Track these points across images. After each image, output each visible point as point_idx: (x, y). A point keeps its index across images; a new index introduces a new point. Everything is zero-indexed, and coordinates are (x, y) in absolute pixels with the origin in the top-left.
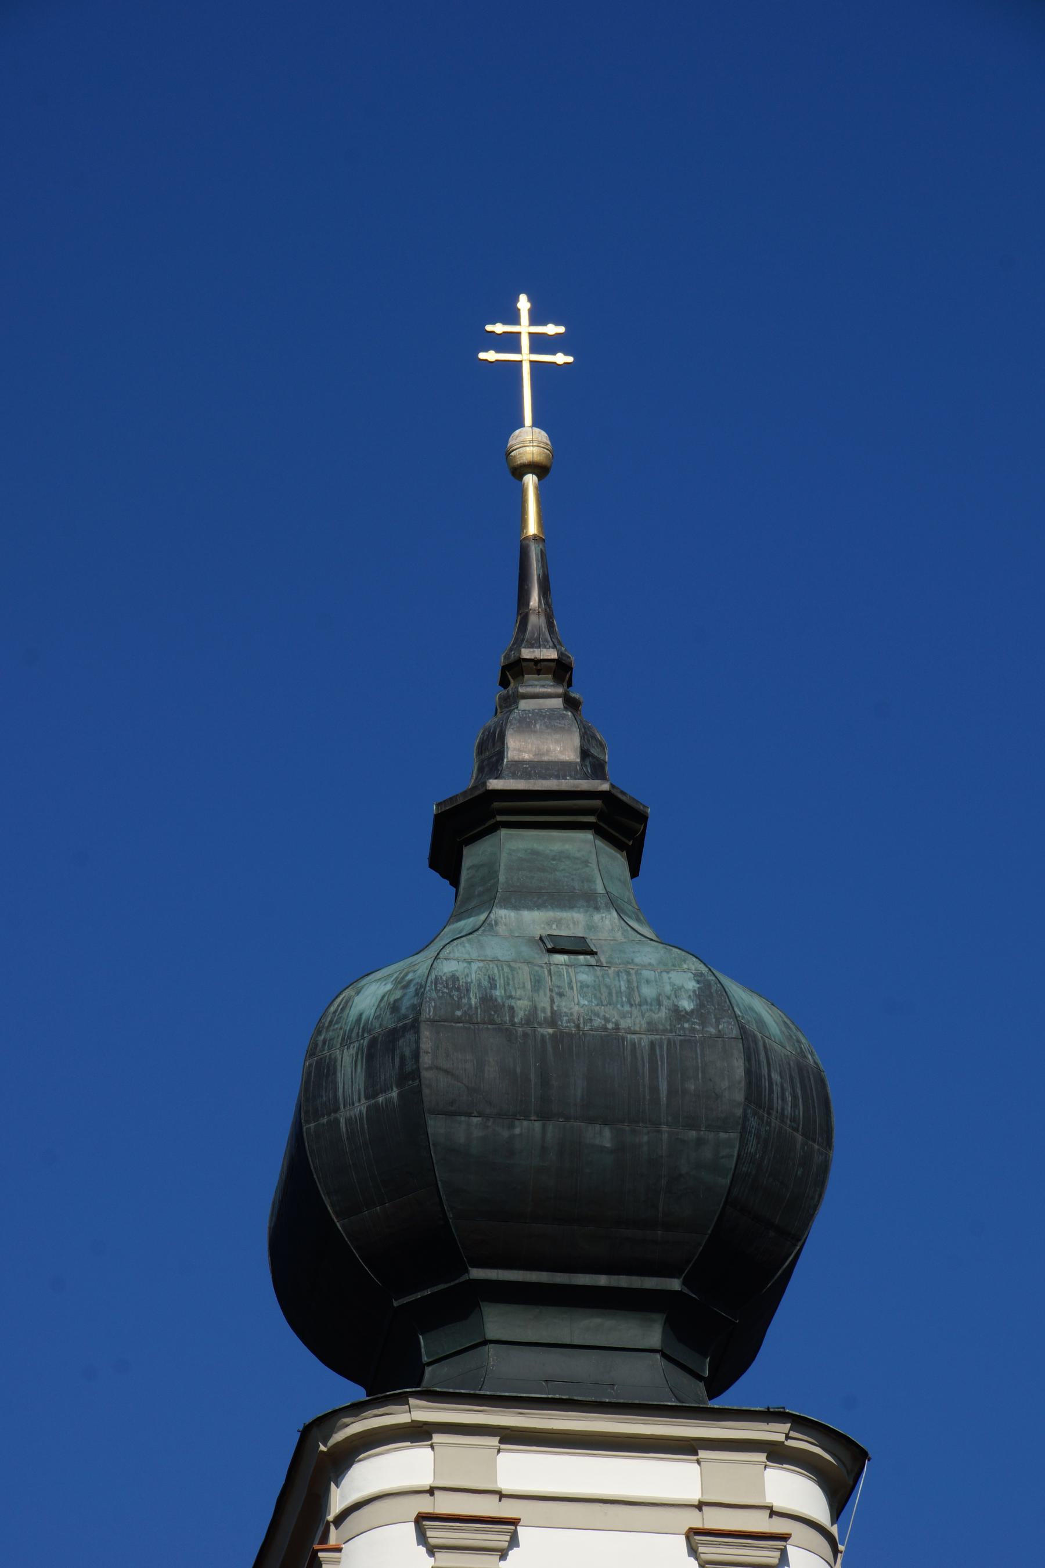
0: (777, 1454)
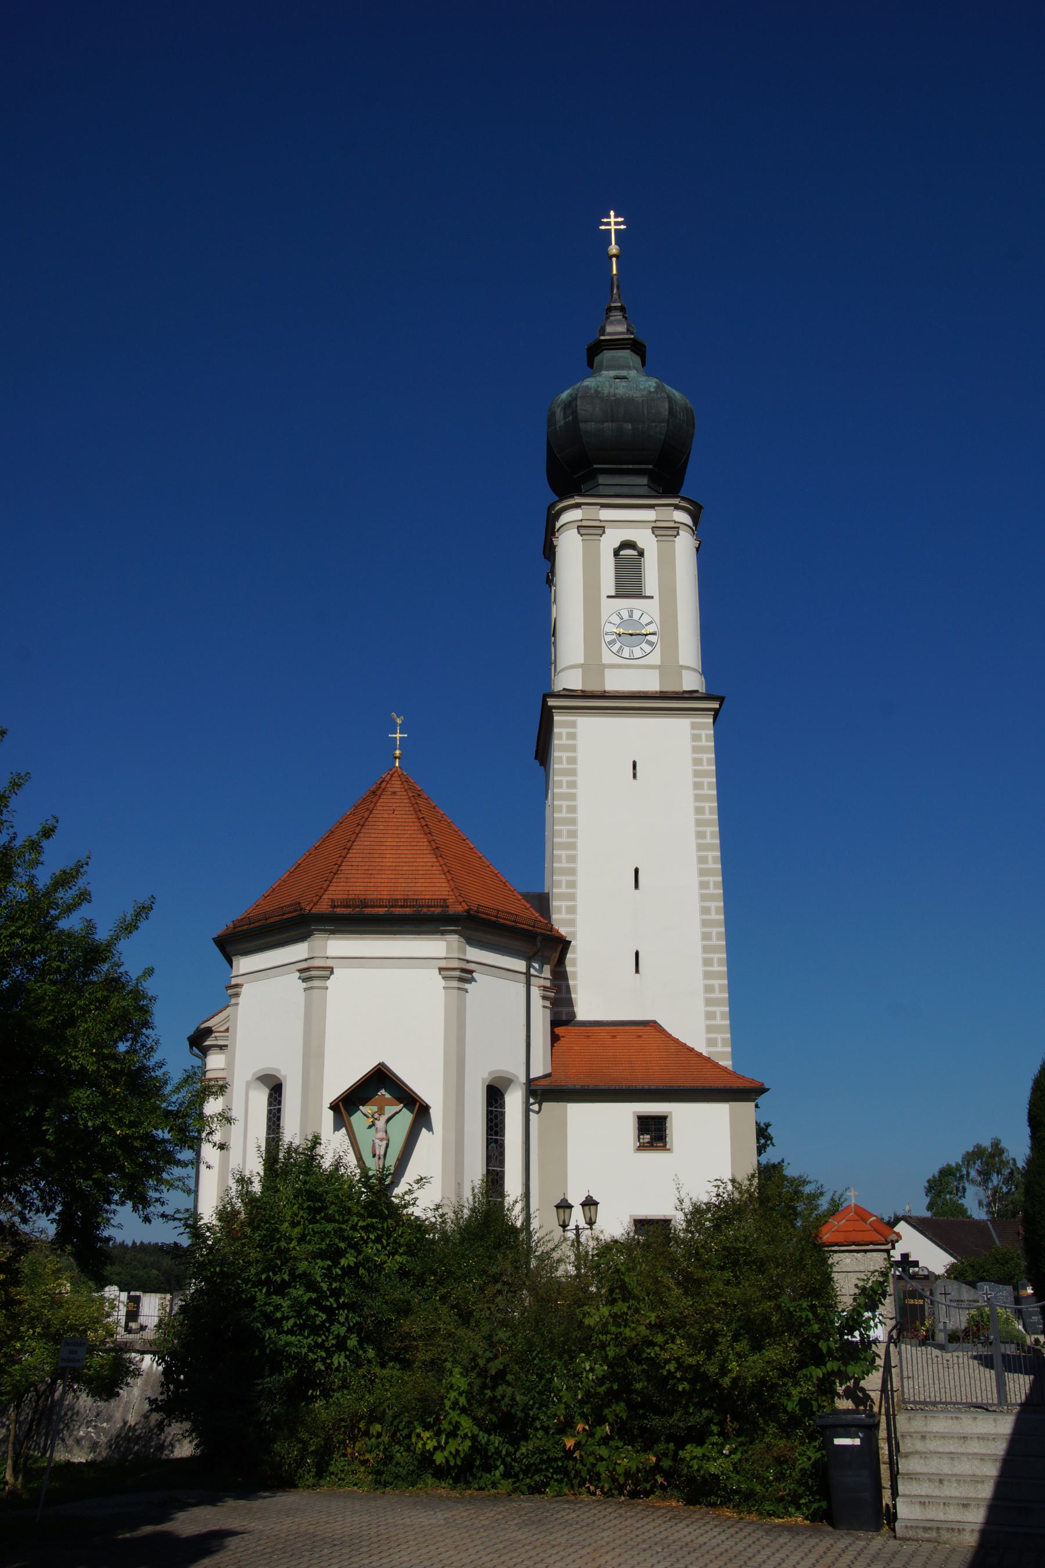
0: (677, 507)
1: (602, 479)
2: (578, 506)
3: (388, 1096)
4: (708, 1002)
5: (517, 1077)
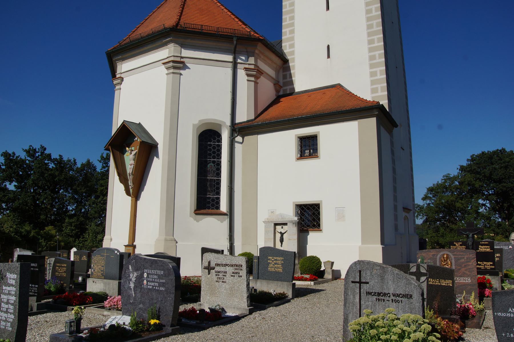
4: (372, 66)
5: (225, 123)
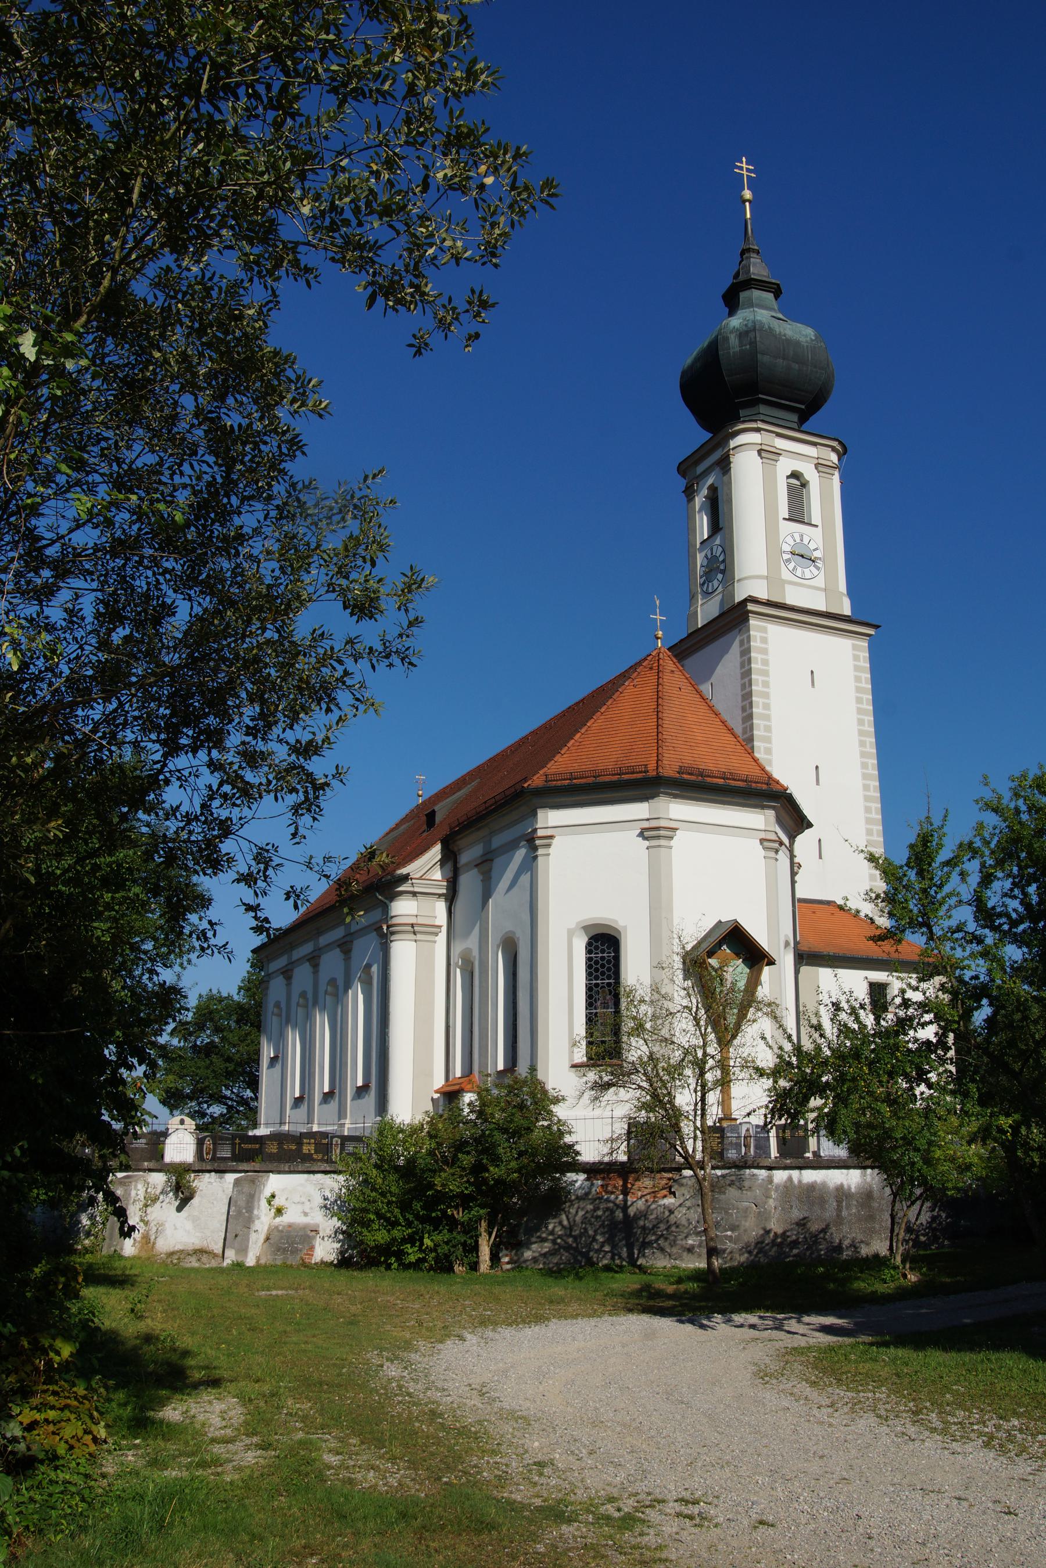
0: (834, 449)
1: (763, 409)
2: (758, 430)
3: (728, 951)
